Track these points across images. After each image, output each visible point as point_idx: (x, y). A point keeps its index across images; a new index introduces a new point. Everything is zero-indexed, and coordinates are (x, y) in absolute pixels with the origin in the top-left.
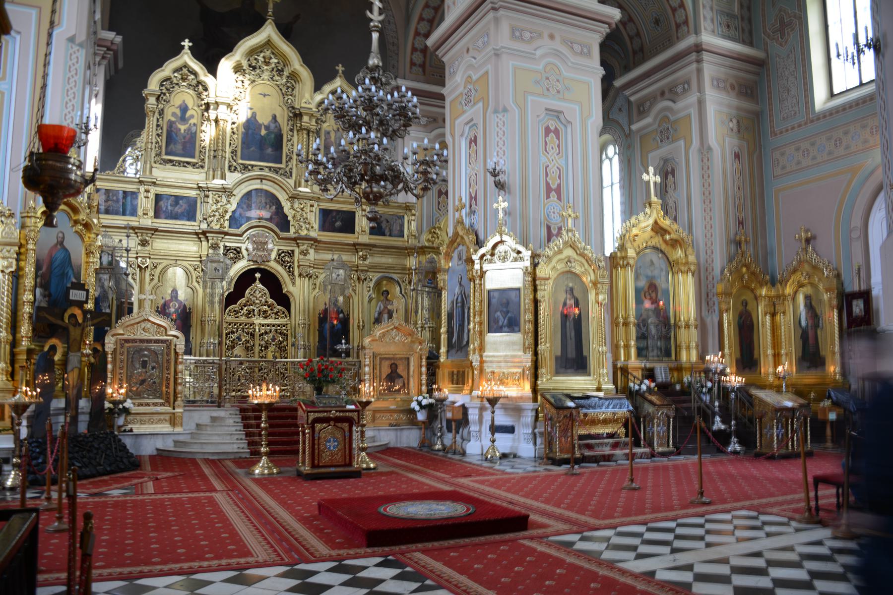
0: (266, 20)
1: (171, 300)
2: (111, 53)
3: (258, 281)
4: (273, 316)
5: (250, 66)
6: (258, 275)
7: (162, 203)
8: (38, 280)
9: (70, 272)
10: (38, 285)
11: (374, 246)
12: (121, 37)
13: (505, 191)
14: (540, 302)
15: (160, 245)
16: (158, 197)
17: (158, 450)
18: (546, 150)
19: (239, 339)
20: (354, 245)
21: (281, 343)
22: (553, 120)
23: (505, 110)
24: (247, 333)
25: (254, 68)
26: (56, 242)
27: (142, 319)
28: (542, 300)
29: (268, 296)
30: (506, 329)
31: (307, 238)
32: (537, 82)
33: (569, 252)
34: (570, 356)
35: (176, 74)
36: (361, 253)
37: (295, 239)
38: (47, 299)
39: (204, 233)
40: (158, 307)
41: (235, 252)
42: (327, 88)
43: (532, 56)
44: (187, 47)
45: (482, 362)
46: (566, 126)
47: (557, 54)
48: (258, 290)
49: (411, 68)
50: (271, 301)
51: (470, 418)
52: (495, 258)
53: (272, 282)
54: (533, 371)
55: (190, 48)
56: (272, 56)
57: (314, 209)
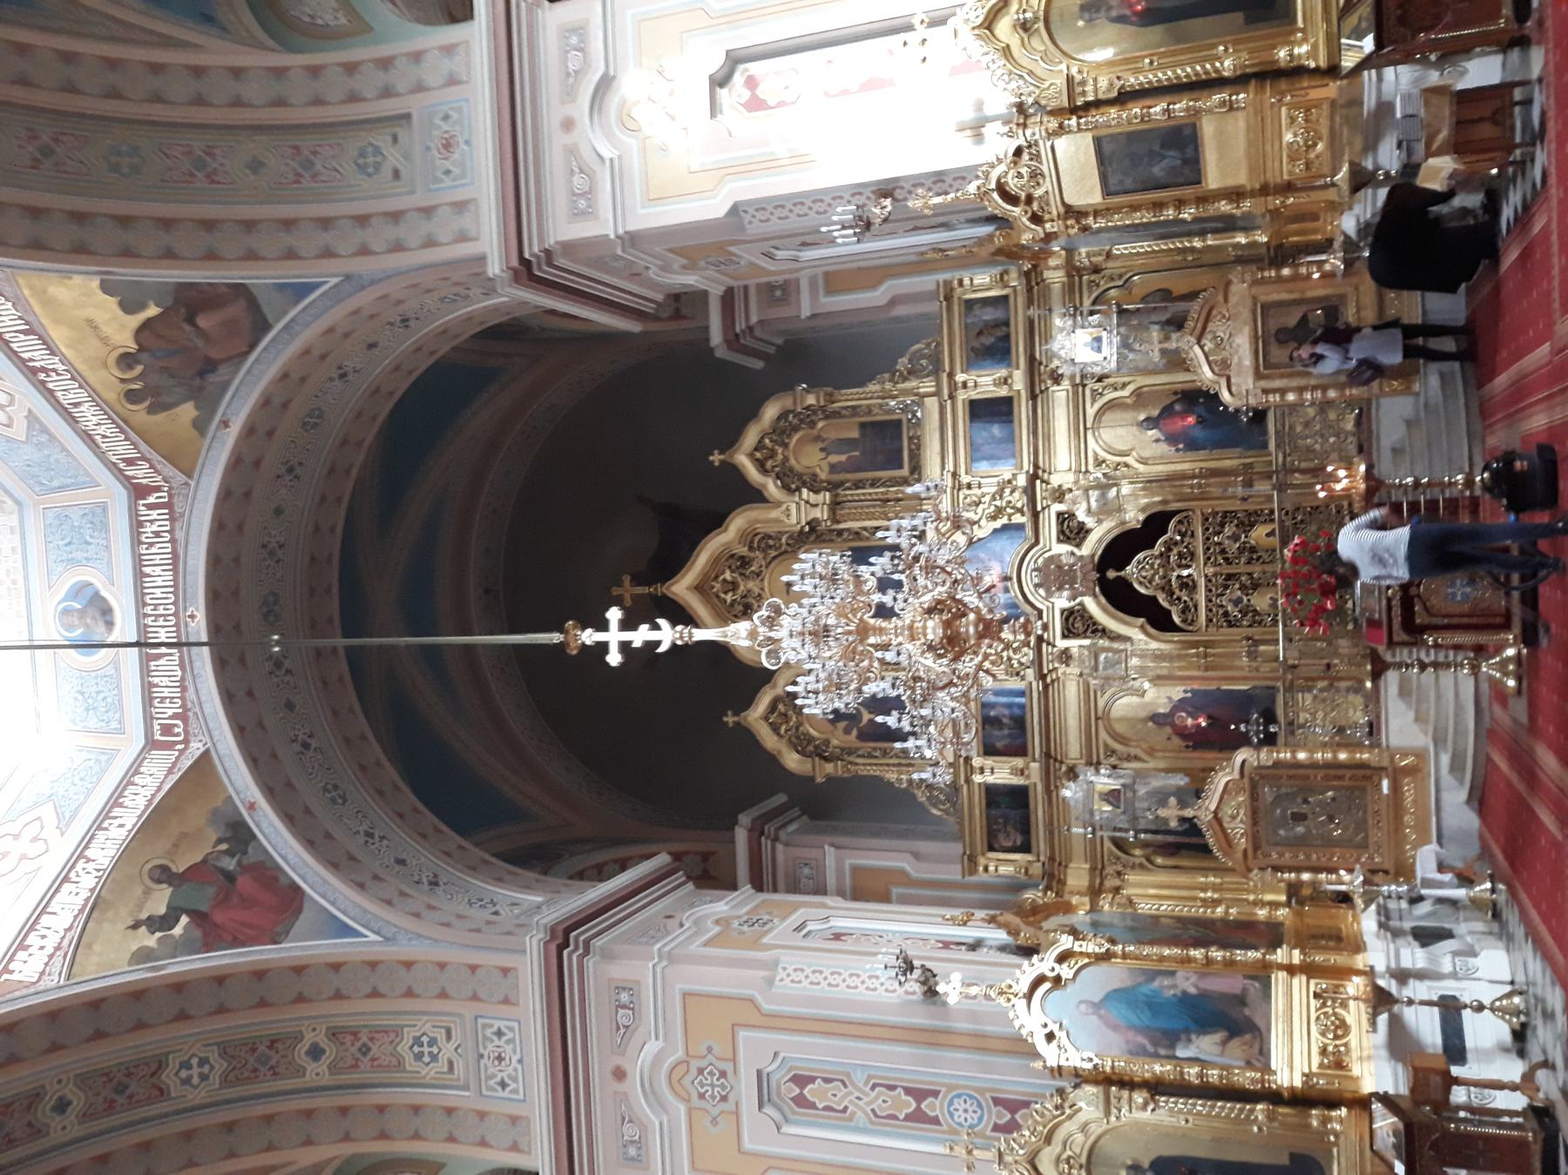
0: (665, 597)
3: (1122, 573)
4: (1187, 540)
6: (1111, 574)
7: (999, 745)
8: (1162, 1052)
9: (1145, 989)
10: (1170, 1053)
11: (1032, 362)
12: (740, 817)
13: (894, 189)
14: (1122, 87)
16: (989, 750)
17: (1469, 801)
19: (1237, 602)
20: (1033, 397)
21: (1242, 523)
24: (1226, 587)
26: (1094, 1018)
27: (1215, 824)
28: (1118, 84)
31: (1030, 491)
33: (1004, 27)
35: (782, 732)
36: (1049, 382)
37: (1035, 515)
38: (1193, 1037)
39: (1042, 677)
40: (1187, 747)
41: (1071, 619)
43: (616, 163)
44: (736, 719)
45: (1265, 190)
48: (1138, 572)
49: (684, 317)
50: (1159, 547)
52: (1038, 192)
53: (1122, 548)
54: (1283, 84)
56: (721, 578)
57: (975, 481)
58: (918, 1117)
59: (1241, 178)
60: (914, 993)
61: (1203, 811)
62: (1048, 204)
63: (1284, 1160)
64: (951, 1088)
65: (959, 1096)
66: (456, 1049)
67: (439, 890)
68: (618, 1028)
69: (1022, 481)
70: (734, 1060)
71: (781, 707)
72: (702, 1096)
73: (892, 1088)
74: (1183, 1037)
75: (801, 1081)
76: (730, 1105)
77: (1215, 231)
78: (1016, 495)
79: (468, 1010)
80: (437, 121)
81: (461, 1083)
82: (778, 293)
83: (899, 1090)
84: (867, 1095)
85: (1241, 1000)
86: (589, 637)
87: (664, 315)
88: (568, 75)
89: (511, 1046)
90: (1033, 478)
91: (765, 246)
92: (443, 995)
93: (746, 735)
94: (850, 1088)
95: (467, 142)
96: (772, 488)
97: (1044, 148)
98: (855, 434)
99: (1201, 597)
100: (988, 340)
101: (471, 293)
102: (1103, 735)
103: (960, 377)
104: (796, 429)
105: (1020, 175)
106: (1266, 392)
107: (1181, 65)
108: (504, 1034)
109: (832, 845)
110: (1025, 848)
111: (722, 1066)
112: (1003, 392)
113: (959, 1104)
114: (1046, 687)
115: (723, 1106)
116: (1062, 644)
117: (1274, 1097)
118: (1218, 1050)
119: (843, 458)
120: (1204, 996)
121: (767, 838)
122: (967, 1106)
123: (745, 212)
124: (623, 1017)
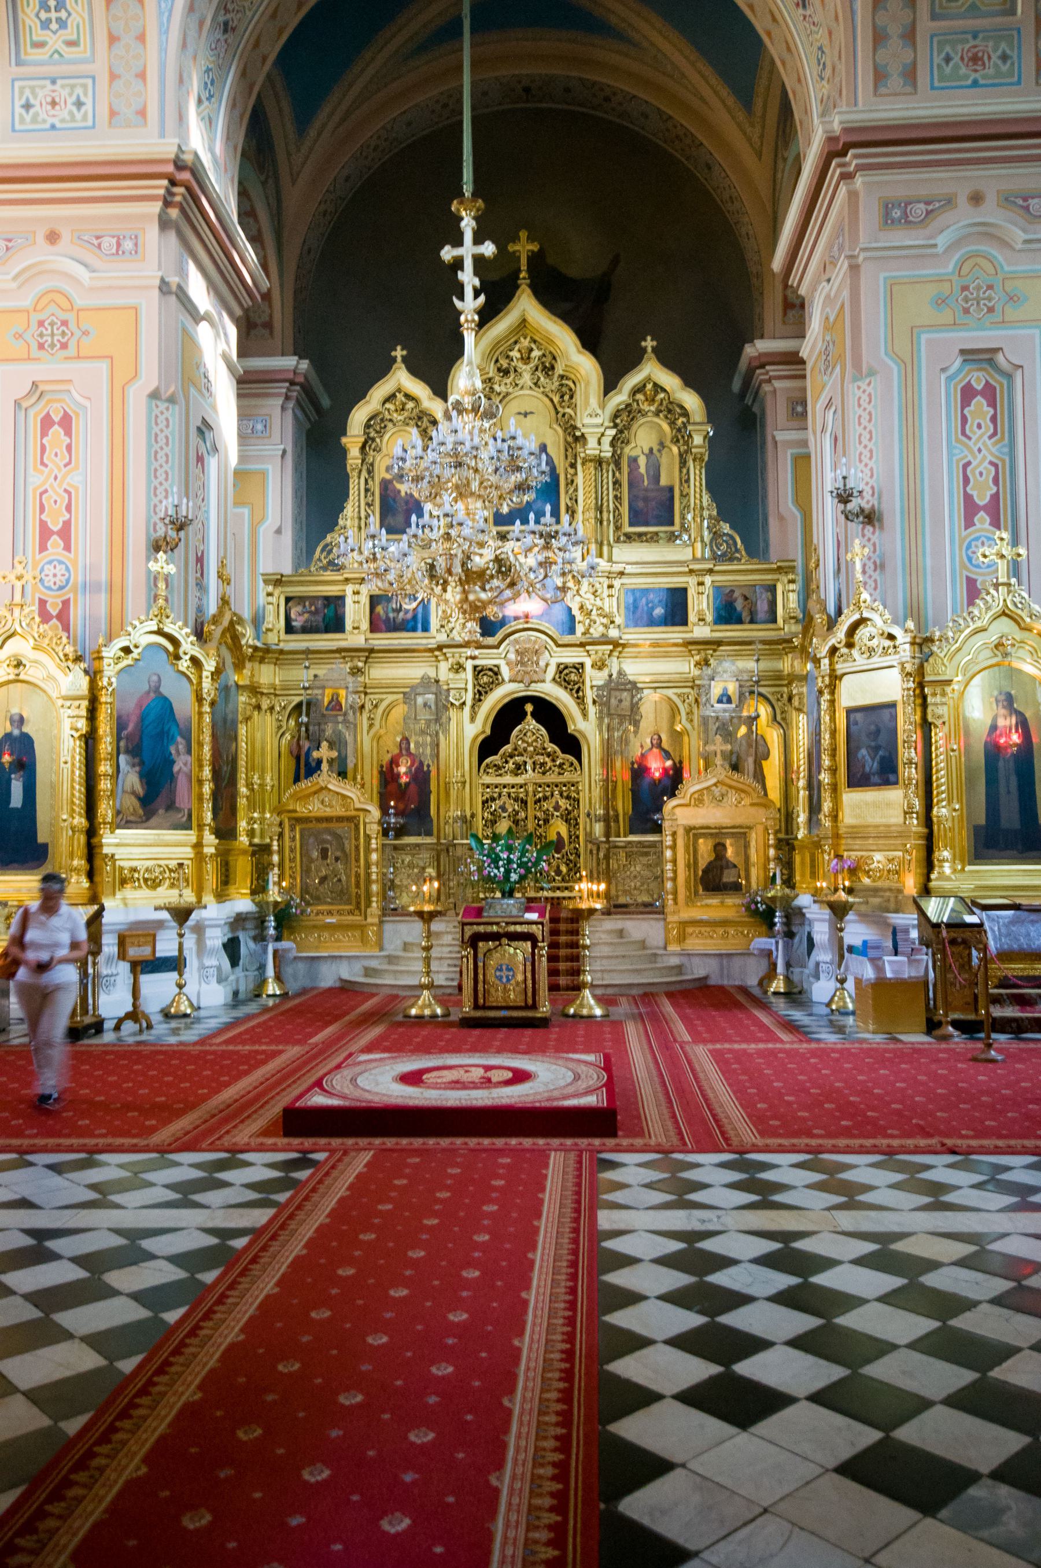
0: (517, 287)
1: (400, 755)
2: (298, 388)
3: (529, 717)
4: (557, 770)
5: (499, 370)
6: (529, 708)
7: (380, 609)
8: (122, 744)
9: (174, 730)
10: (122, 749)
11: (719, 643)
12: (307, 361)
14: (936, 726)
15: (380, 672)
16: (374, 601)
17: (341, 980)
18: (964, 433)
19: (503, 808)
21: (569, 813)
22: (979, 370)
23: (872, 373)
25: (506, 372)
26: (146, 688)
27: (317, 787)
28: (938, 722)
29: (547, 738)
30: (876, 779)
31: (604, 640)
32: (940, 302)
34: (1004, 824)
35: (387, 405)
36: (697, 658)
37: (582, 645)
39: (440, 648)
42: (632, 380)
43: (934, 250)
44: (399, 359)
46: (1009, 376)
47: (987, 233)
49: (785, 314)
50: (551, 747)
51: (817, 938)
52: (855, 652)
54: (923, 854)
55: (404, 359)
56: (533, 346)
58: (45, 533)
59: (848, 818)
60: (155, 531)
61: (326, 778)
62: (845, 661)
63: (41, 839)
64: (75, 562)
65: (67, 569)
66: (57, 51)
67: (218, 34)
68: (98, 238)
69: (613, 633)
70: (78, 357)
71: (410, 405)
72: (41, 323)
73: (68, 508)
74: (137, 760)
75: (66, 422)
76: (35, 352)
77: (811, 797)
78: (601, 629)
79: (100, 67)
80: (1003, 46)
81: (23, 57)
82: (799, 409)
83: (67, 516)
84: (60, 486)
85: (171, 806)
86: (468, 225)
87: (789, 292)
88: (1025, 199)
89: (68, 118)
90: (616, 644)
91: (837, 401)
92: (113, 39)
93: (384, 369)
94: (64, 470)
95: (975, 84)
96: (620, 398)
97: (892, 659)
98: (664, 482)
99: (508, 779)
100: (739, 605)
101: (825, 83)
102: (390, 698)
103: (708, 580)
104: (672, 423)
105: (871, 638)
106: (674, 834)
107: (949, 775)
108: (79, 109)
109: (284, 452)
110: (289, 629)
111: (72, 344)
112: (692, 617)
113: (60, 570)
114: (431, 650)
115: (34, 346)
116: (469, 665)
117: (91, 833)
118: (128, 788)
119: (642, 470)
120: (172, 778)
121: (288, 389)
122: (59, 577)
123: (869, 384)
124: (109, 243)
